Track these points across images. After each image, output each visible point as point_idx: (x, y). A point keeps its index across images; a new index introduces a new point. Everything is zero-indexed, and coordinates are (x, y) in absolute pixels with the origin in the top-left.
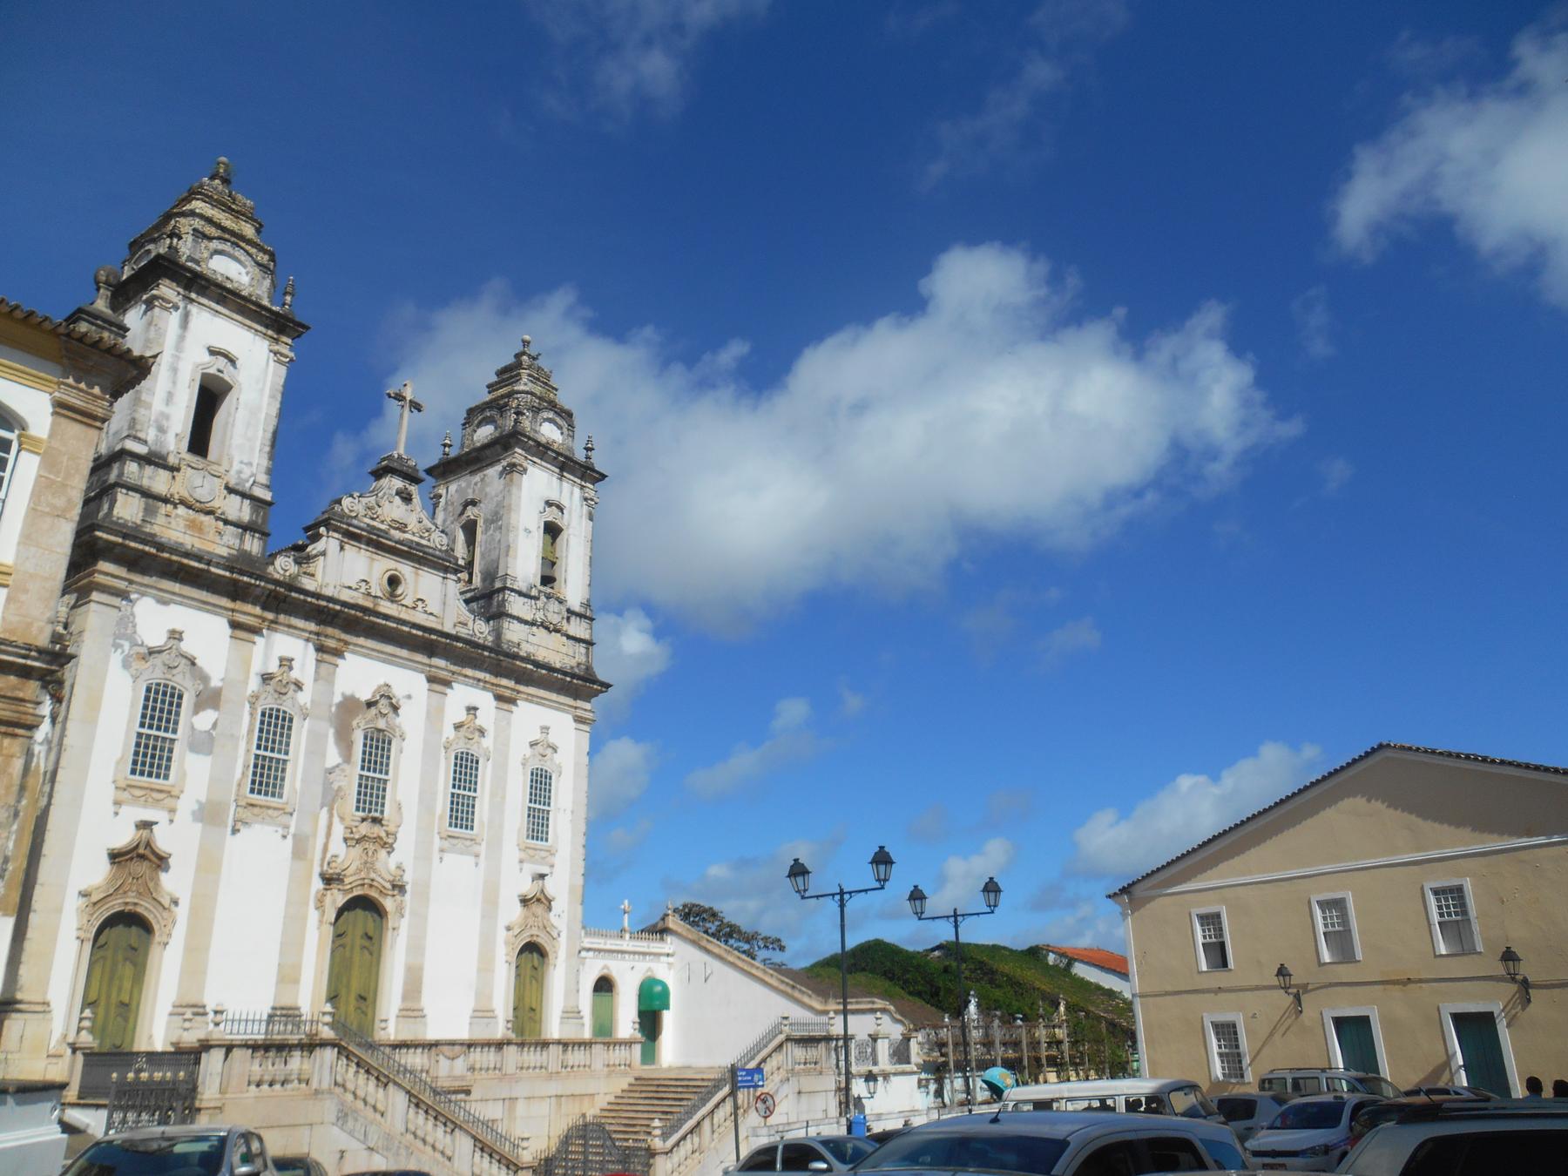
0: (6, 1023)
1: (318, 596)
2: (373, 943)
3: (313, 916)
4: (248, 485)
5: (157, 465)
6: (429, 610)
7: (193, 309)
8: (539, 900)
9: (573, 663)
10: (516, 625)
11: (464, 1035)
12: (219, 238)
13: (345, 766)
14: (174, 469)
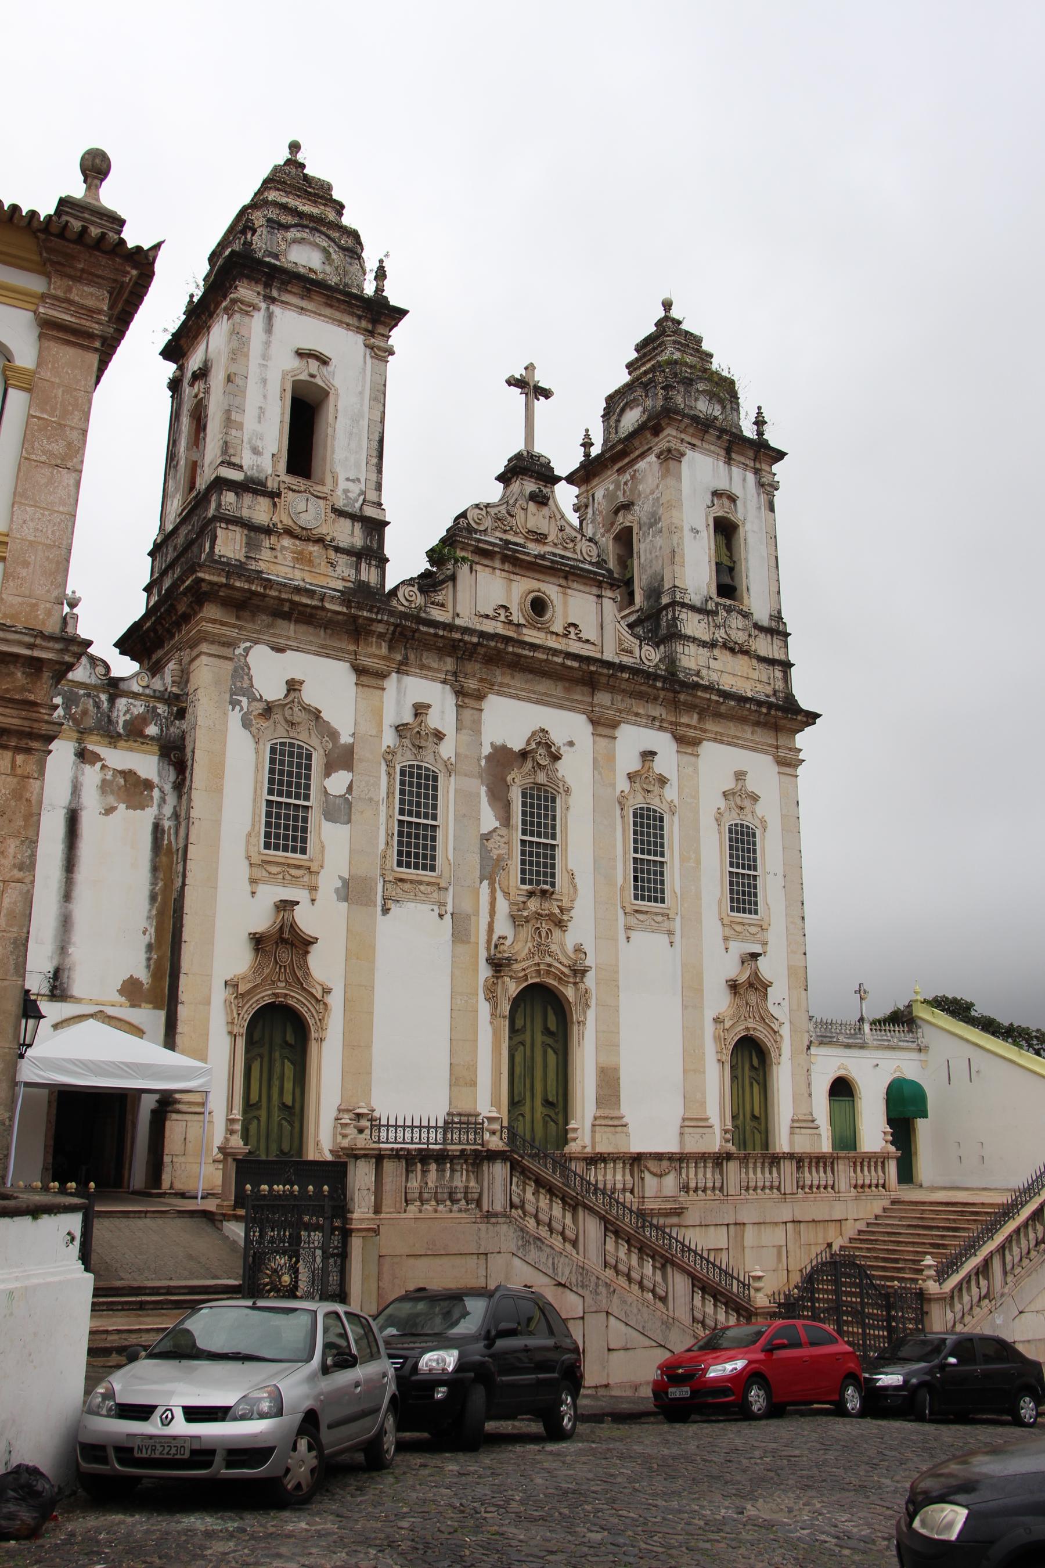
0: (168, 1124)
1: (450, 627)
3: (484, 1008)
4: (358, 505)
5: (256, 492)
6: (584, 635)
7: (276, 309)
8: (751, 985)
9: (769, 690)
10: (692, 649)
11: (670, 1145)
12: (296, 225)
13: (503, 831)
14: (274, 495)
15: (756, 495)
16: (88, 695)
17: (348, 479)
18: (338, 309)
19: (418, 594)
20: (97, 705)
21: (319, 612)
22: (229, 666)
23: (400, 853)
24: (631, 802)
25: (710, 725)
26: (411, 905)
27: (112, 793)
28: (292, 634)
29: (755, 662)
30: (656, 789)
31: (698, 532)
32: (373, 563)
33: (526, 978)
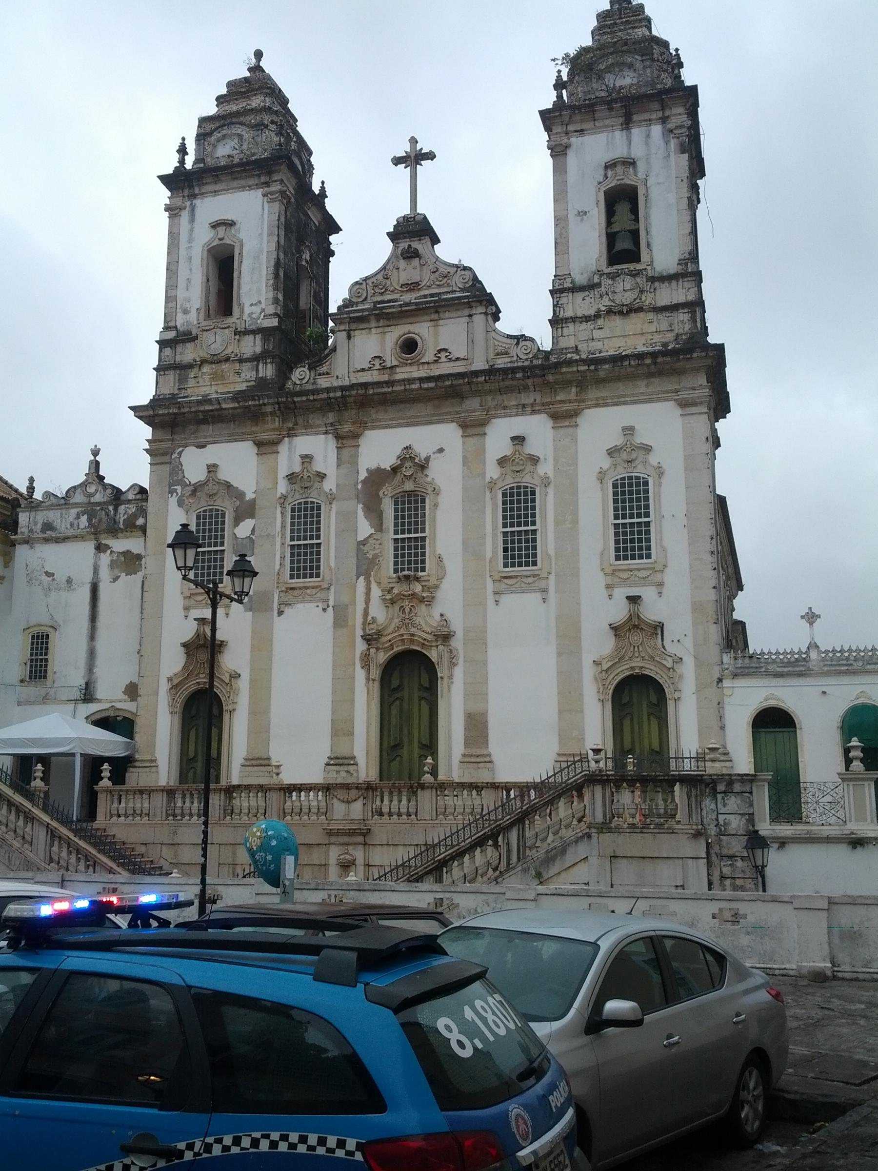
2: (430, 691)
3: (360, 675)
5: (184, 341)
7: (198, 202)
13: (377, 536)
15: (663, 144)
16: (102, 509)
17: (252, 305)
18: (241, 178)
19: (308, 372)
20: (107, 515)
21: (224, 412)
22: (167, 468)
23: (292, 569)
24: (499, 485)
25: (593, 394)
26: (300, 606)
27: (117, 567)
28: (211, 432)
29: (651, 315)
30: (529, 468)
31: (585, 213)
32: (269, 361)
33: (392, 647)
